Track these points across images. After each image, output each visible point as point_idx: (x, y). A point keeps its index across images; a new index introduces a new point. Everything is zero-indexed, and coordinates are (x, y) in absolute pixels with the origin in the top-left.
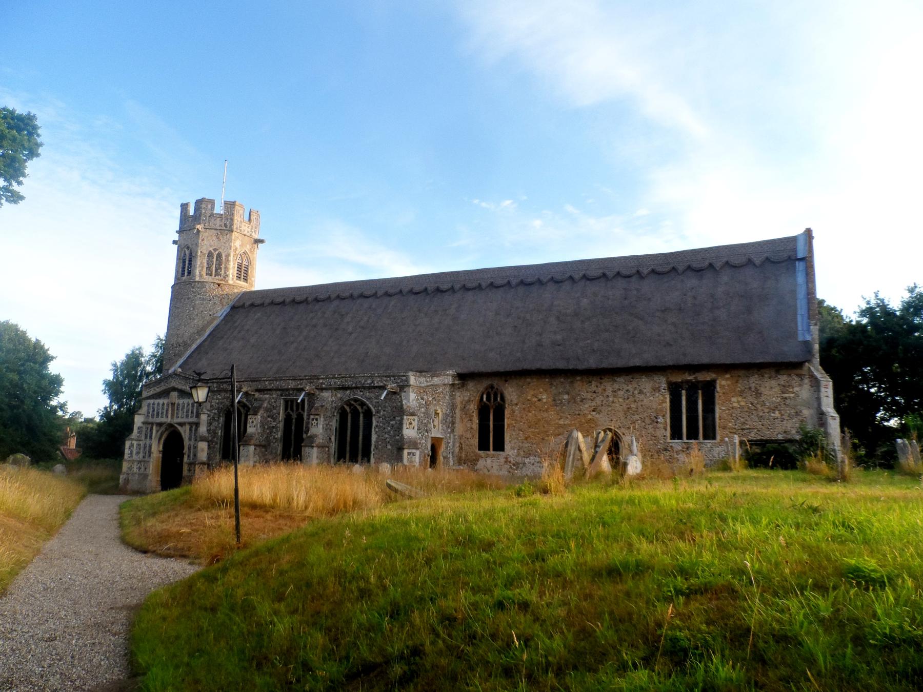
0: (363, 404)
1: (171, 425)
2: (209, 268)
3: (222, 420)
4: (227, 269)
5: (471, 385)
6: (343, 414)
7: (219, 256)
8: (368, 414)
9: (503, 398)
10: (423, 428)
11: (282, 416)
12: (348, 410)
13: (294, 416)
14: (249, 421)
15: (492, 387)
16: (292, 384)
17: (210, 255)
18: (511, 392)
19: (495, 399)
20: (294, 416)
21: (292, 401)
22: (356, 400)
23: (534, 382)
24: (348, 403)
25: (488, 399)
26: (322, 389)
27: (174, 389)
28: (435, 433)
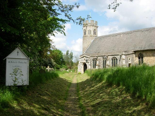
0: (116, 58)
1: (84, 63)
2: (89, 33)
3: (93, 61)
4: (92, 33)
5: (137, 53)
6: (112, 59)
7: (90, 31)
8: (117, 59)
9: (143, 55)
10: (126, 62)
11: (102, 60)
12: (113, 59)
13: (104, 60)
14: (97, 62)
15: (141, 53)
16: (104, 55)
17: (89, 31)
18: (144, 54)
19: (141, 56)
20: (104, 60)
21: (104, 58)
22: (114, 57)
23: (149, 52)
24: (113, 58)
25: (140, 56)
26: (108, 56)
27: (84, 56)
28: (130, 62)
